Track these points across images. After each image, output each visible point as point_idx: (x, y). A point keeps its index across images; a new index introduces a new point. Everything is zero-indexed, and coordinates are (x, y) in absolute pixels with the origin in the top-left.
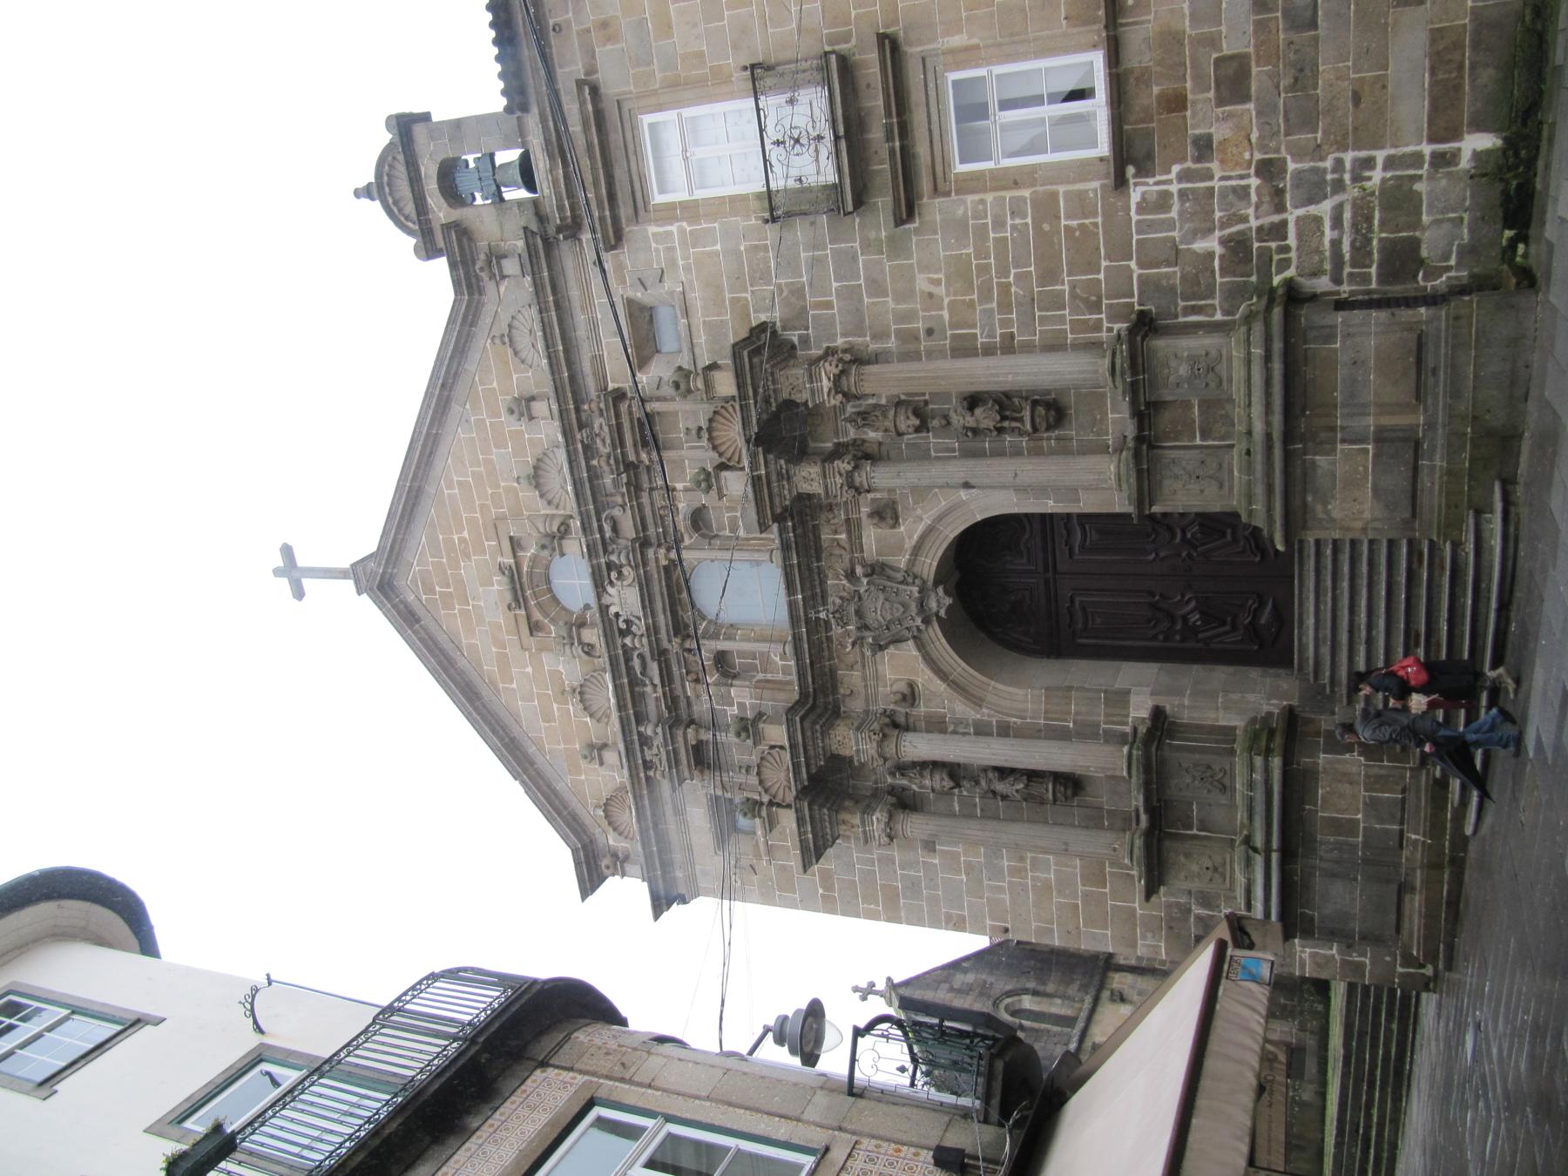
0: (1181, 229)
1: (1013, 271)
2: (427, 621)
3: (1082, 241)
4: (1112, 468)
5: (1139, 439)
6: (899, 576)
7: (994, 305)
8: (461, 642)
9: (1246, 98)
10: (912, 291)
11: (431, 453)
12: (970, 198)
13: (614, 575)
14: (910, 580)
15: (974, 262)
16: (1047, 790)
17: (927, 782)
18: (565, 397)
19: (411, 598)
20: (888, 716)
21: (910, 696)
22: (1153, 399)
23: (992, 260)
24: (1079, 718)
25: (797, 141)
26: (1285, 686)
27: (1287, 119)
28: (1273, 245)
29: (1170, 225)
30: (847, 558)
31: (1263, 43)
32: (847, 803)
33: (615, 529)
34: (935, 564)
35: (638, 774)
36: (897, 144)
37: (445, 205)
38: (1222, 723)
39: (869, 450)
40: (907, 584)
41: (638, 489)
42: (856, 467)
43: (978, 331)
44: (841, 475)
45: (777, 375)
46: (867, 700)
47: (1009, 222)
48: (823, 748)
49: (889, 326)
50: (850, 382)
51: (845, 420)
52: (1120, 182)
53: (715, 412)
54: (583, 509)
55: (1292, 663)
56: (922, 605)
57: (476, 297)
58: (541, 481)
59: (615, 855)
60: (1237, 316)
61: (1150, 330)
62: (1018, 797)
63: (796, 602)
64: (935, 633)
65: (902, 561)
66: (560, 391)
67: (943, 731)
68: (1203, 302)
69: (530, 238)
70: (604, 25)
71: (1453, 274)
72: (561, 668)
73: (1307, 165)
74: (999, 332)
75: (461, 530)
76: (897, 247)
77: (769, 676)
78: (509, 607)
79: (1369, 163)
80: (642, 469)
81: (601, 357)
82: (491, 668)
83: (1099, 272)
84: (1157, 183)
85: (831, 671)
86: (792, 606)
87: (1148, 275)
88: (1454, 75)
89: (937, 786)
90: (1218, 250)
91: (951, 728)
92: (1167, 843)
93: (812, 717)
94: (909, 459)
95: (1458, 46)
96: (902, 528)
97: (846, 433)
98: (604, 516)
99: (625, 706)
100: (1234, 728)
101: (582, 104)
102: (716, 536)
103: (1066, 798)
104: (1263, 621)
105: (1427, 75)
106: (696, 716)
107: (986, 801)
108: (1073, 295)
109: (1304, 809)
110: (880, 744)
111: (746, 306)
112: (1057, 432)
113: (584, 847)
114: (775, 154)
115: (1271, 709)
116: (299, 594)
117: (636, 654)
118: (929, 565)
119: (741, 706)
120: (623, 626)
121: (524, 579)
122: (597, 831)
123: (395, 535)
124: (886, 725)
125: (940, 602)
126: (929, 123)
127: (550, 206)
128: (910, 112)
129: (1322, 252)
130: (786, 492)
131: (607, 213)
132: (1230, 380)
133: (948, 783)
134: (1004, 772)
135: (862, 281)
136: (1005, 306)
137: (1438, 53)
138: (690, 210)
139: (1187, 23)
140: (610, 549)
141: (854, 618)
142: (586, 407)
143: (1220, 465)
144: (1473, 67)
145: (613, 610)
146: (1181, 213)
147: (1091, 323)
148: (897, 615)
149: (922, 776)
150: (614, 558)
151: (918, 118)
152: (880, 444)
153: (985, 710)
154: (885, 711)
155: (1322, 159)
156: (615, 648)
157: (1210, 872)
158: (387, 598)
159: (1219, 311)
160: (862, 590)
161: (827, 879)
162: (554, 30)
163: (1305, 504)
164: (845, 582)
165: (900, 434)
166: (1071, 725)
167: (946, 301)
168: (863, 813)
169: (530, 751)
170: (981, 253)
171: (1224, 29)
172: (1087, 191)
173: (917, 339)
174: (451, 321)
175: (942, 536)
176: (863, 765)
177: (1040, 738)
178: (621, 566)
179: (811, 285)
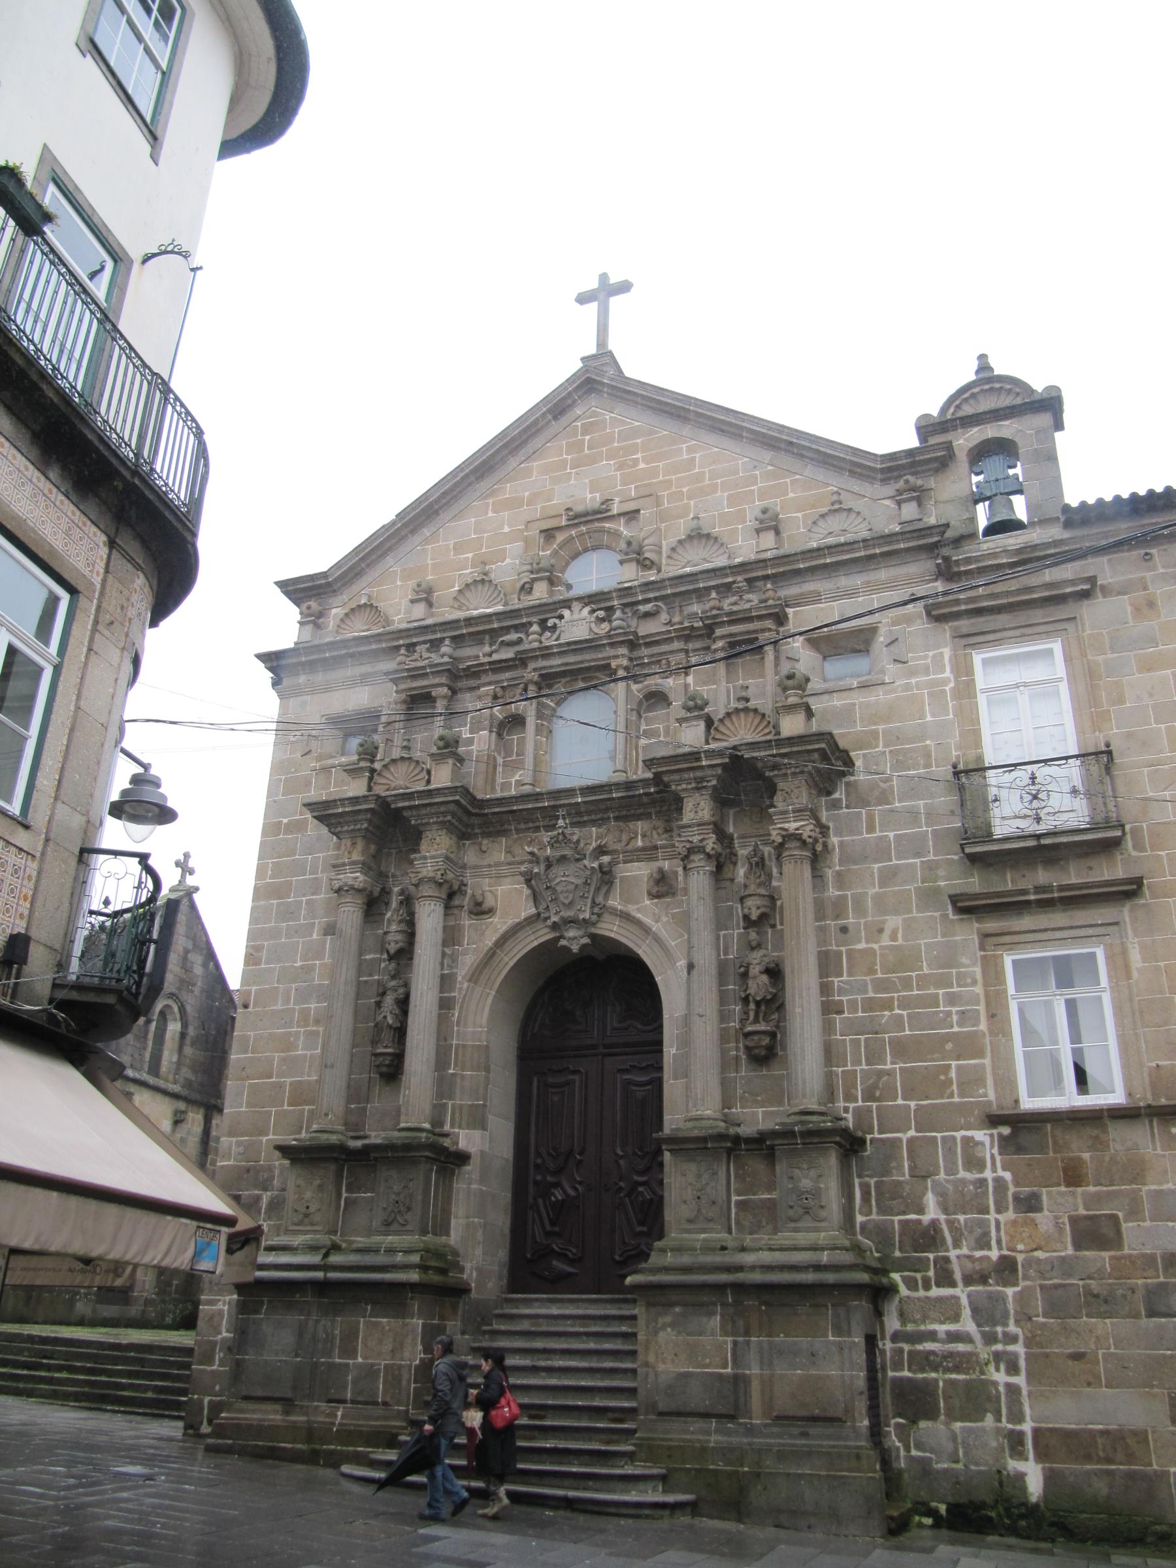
0: (947, 1181)
1: (905, 1013)
2: (555, 427)
3: (936, 1082)
4: (708, 1112)
5: (737, 1139)
6: (600, 899)
7: (871, 995)
8: (535, 460)
9: (1078, 1246)
10: (885, 912)
11: (723, 431)
12: (978, 970)
13: (601, 614)
14: (596, 910)
15: (914, 974)
16: (386, 1047)
17: (394, 927)
18: (779, 565)
19: (578, 411)
20: (460, 888)
21: (480, 910)
22: (777, 1153)
23: (916, 992)
24: (458, 1080)
25: (1035, 797)
26: (490, 1285)
27: (1056, 1287)
28: (931, 1273)
29: (952, 1170)
30: (618, 847)
31: (1133, 1263)
32: (373, 847)
33: (647, 615)
34: (612, 935)
35: (402, 638)
36: (1032, 897)
37: (971, 446)
38: (453, 1222)
39: (725, 869)
40: (592, 907)
41: (687, 638)
42: (709, 856)
43: (845, 978)
44: (701, 841)
45: (801, 777)
46: (476, 867)
47: (954, 1009)
48: (428, 824)
49: (850, 889)
50: (793, 849)
51: (756, 845)
52: (994, 1120)
53: (763, 715)
54: (667, 583)
55: (513, 1292)
56: (571, 922)
57: (879, 476)
58: (695, 542)
59: (320, 615)
60: (860, 1237)
61: (847, 1150)
62: (380, 1018)
64: (543, 935)
65: (615, 902)
66: (786, 560)
67: (445, 943)
68: (874, 1203)
69: (938, 530)
70: (1151, 604)
71: (902, 1453)
72: (508, 561)
73: (1011, 1306)
74: (844, 999)
75: (646, 460)
76: (929, 897)
77: (500, 769)
78: (568, 509)
79: (1013, 1369)
80: (707, 642)
81: (819, 601)
82: (508, 490)
83: (904, 1099)
84: (992, 1156)
85: (506, 831)
86: (570, 792)
87: (900, 1148)
88: (1101, 1454)
89: (390, 937)
90: (926, 1218)
91: (448, 951)
92: (333, 1167)
93: (460, 813)
94: (716, 909)
95: (1130, 1458)
96: (648, 902)
97: (743, 846)
98: (660, 604)
99: (471, 625)
100: (448, 1234)
101: (1073, 582)
102: (640, 716)
103: (378, 1066)
104: (555, 1263)
105: (1101, 1427)
106: (459, 696)
107: (375, 986)
108: (880, 1074)
109: (367, 1304)
110: (432, 880)
111: (870, 746)
112: (744, 1057)
113: (329, 584)
114: (1023, 774)
115: (467, 1271)
116: (583, 299)
117: (522, 636)
118: (611, 929)
119: (470, 741)
120: (550, 623)
121: (597, 524)
122: (345, 597)
123: (643, 396)
124: (451, 887)
125: (575, 940)
126: (1054, 929)
127: (970, 550)
128: (1064, 911)
129: (924, 1322)
130: (684, 786)
131: (963, 607)
132: (796, 1230)
133: (393, 948)
134: (404, 1004)
135: (895, 862)
136: (870, 1005)
137: (1123, 1438)
138: (966, 690)
139: (1153, 1187)
140: (627, 610)
141: (558, 854)
142: (769, 586)
143: (710, 1220)
144: (1109, 1473)
145: (566, 613)
146: (963, 1181)
147: (853, 1091)
148: (561, 897)
149: (400, 922)
150: (618, 614)
151: (1059, 918)
152: (732, 880)
153: (466, 985)
154: (465, 885)
155: (1017, 1322)
156: (528, 615)
157: (304, 1210)
158: (578, 387)
159: (864, 1219)
160: (586, 862)
161: (297, 827)
162: (1147, 554)
163: (672, 1305)
164: (594, 845)
165: (742, 900)
166: (451, 1071)
167: (875, 946)
168: (363, 864)
169: (425, 530)
170: (923, 981)
171: (1148, 1224)
172: (985, 1087)
173: (837, 917)
174: (856, 451)
176: (411, 862)
177: (438, 1040)
178: (610, 621)
179: (891, 811)
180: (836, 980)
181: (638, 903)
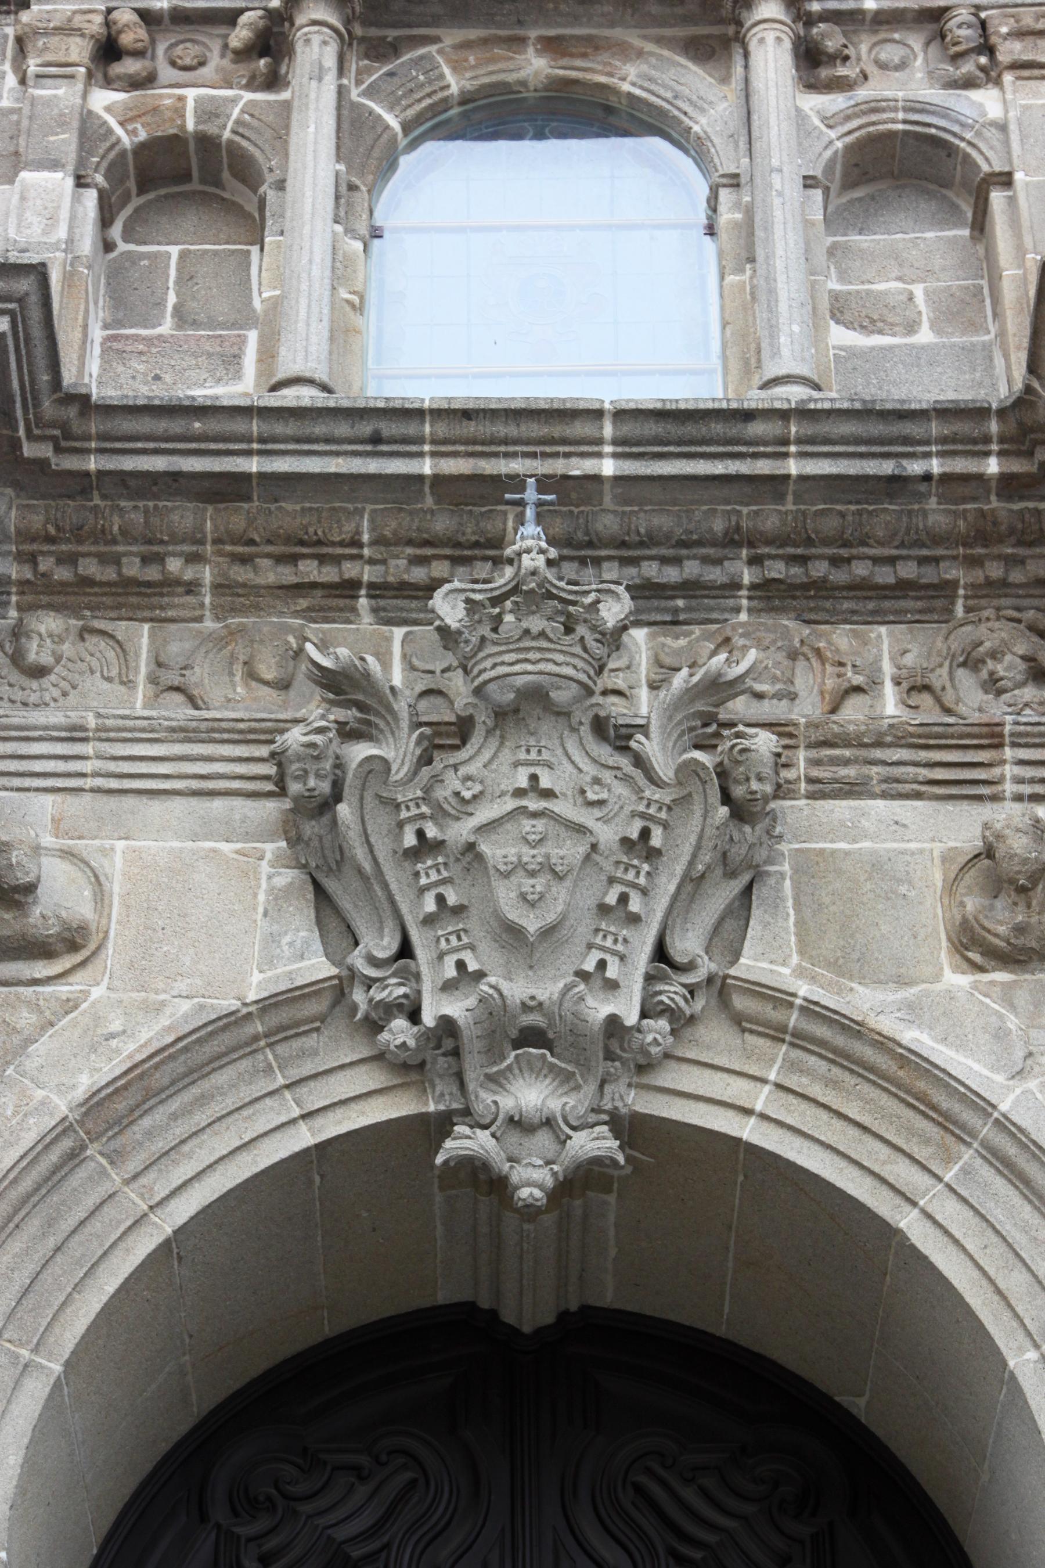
14: (672, 992)
34: (748, 1131)
56: (532, 1037)
63: (591, 446)
85: (170, 584)
96: (963, 981)
175: (902, 1172)
181: (902, 982)
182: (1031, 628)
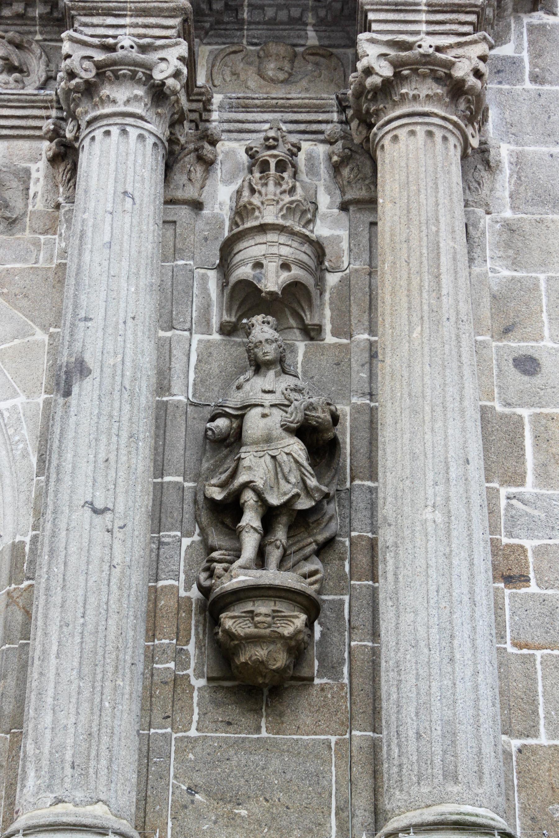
39: (180, 178)
44: (143, 49)
49: (544, 265)
112: (199, 683)
180: (504, 492)
182: (10, 42)
